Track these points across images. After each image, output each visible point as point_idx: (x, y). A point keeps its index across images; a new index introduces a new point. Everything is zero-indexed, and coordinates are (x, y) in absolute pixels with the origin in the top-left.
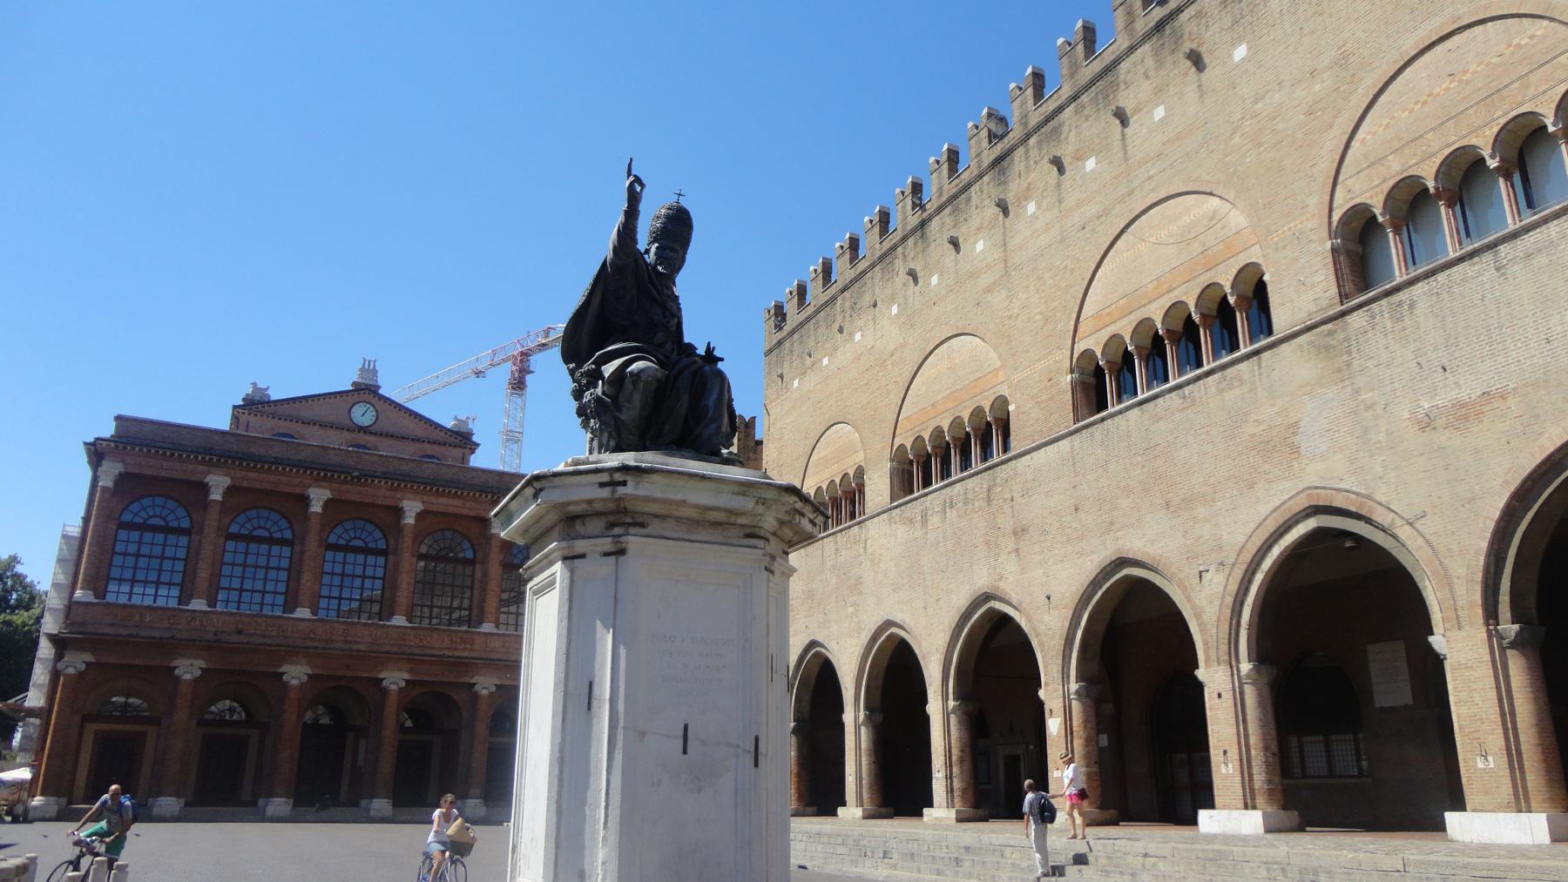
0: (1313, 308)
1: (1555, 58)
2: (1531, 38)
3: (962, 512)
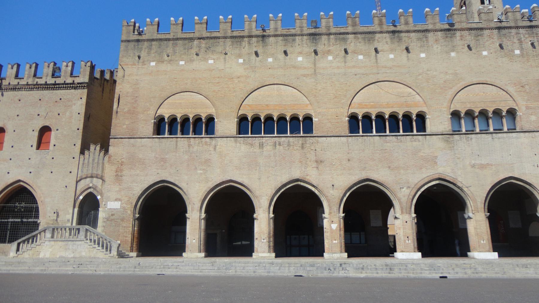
0: (444, 130)
1: (507, 101)
2: (502, 94)
3: (287, 148)
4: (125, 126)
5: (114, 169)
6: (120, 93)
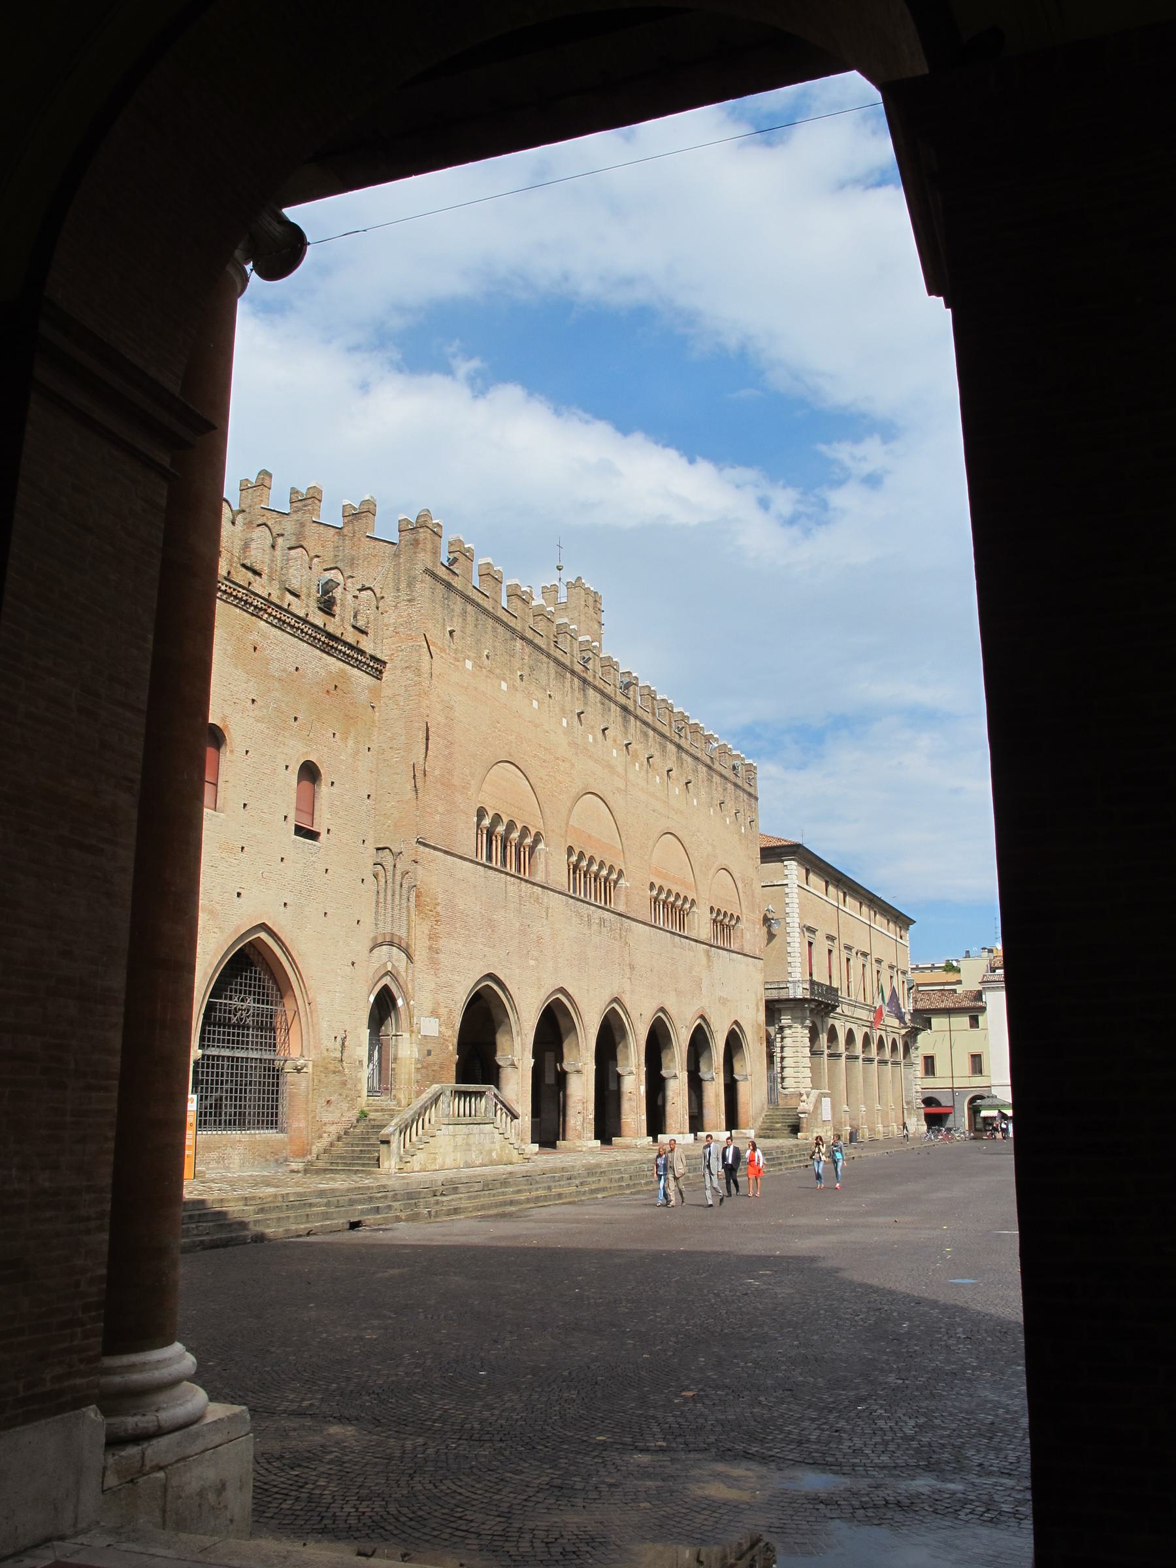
4: (438, 817)
5: (427, 932)
6: (426, 719)
